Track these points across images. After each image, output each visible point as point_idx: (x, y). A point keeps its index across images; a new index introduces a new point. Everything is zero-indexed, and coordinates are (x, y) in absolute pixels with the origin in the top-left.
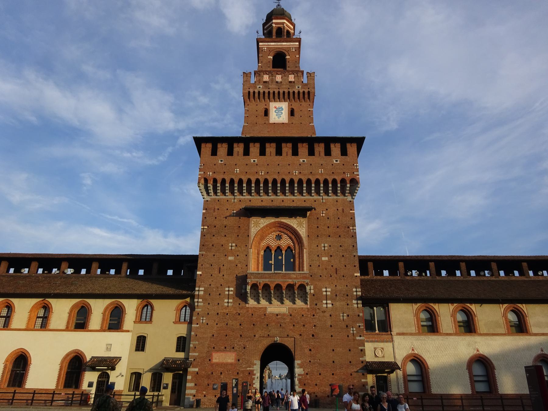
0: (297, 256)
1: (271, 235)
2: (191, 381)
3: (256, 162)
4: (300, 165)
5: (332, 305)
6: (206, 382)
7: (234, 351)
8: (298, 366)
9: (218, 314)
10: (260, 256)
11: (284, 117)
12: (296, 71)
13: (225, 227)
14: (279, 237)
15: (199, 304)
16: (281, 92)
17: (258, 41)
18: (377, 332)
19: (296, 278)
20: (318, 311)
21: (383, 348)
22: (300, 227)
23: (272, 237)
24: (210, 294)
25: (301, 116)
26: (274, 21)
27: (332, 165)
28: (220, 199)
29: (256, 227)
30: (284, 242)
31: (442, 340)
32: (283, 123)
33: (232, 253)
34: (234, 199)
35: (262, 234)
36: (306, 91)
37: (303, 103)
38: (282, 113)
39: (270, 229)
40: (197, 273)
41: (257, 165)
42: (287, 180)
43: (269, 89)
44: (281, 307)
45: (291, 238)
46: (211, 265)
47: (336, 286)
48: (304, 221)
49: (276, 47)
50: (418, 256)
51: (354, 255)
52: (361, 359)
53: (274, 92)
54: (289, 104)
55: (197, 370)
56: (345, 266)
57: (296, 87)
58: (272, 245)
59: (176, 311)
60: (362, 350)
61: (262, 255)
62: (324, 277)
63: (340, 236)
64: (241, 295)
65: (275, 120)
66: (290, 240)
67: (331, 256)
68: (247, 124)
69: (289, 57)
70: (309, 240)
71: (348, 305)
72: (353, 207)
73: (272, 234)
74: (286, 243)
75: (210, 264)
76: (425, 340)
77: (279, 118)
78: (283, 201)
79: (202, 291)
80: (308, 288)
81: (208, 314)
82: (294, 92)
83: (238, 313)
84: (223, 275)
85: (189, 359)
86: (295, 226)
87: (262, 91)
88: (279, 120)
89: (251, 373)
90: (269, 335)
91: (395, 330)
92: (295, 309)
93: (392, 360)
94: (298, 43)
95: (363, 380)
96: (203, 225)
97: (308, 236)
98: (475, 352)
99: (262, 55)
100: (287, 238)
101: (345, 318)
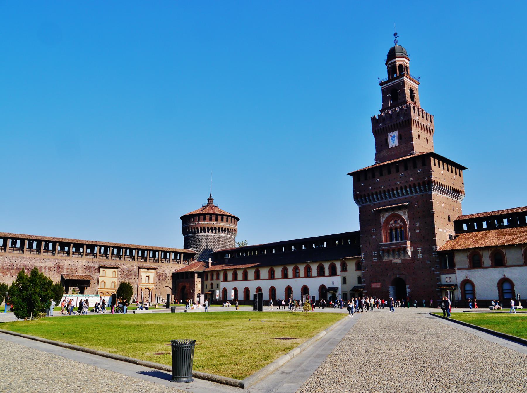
4: (400, 178)
5: (422, 256)
10: (388, 234)
14: (395, 222)
15: (364, 261)
16: (392, 124)
20: (415, 260)
21: (450, 277)
26: (389, 62)
27: (417, 174)
31: (483, 271)
33: (374, 234)
35: (387, 221)
38: (395, 139)
42: (395, 188)
43: (386, 124)
52: (437, 283)
53: (389, 126)
55: (366, 291)
56: (428, 234)
59: (355, 266)
60: (437, 279)
61: (389, 233)
62: (418, 242)
63: (425, 217)
67: (421, 229)
71: (430, 255)
76: (473, 271)
78: (395, 201)
84: (372, 246)
86: (402, 215)
87: (382, 128)
88: (394, 144)
89: (388, 292)
91: (457, 267)
92: (404, 260)
93: (455, 283)
95: (438, 294)
96: (360, 221)
98: (503, 277)
101: (429, 262)
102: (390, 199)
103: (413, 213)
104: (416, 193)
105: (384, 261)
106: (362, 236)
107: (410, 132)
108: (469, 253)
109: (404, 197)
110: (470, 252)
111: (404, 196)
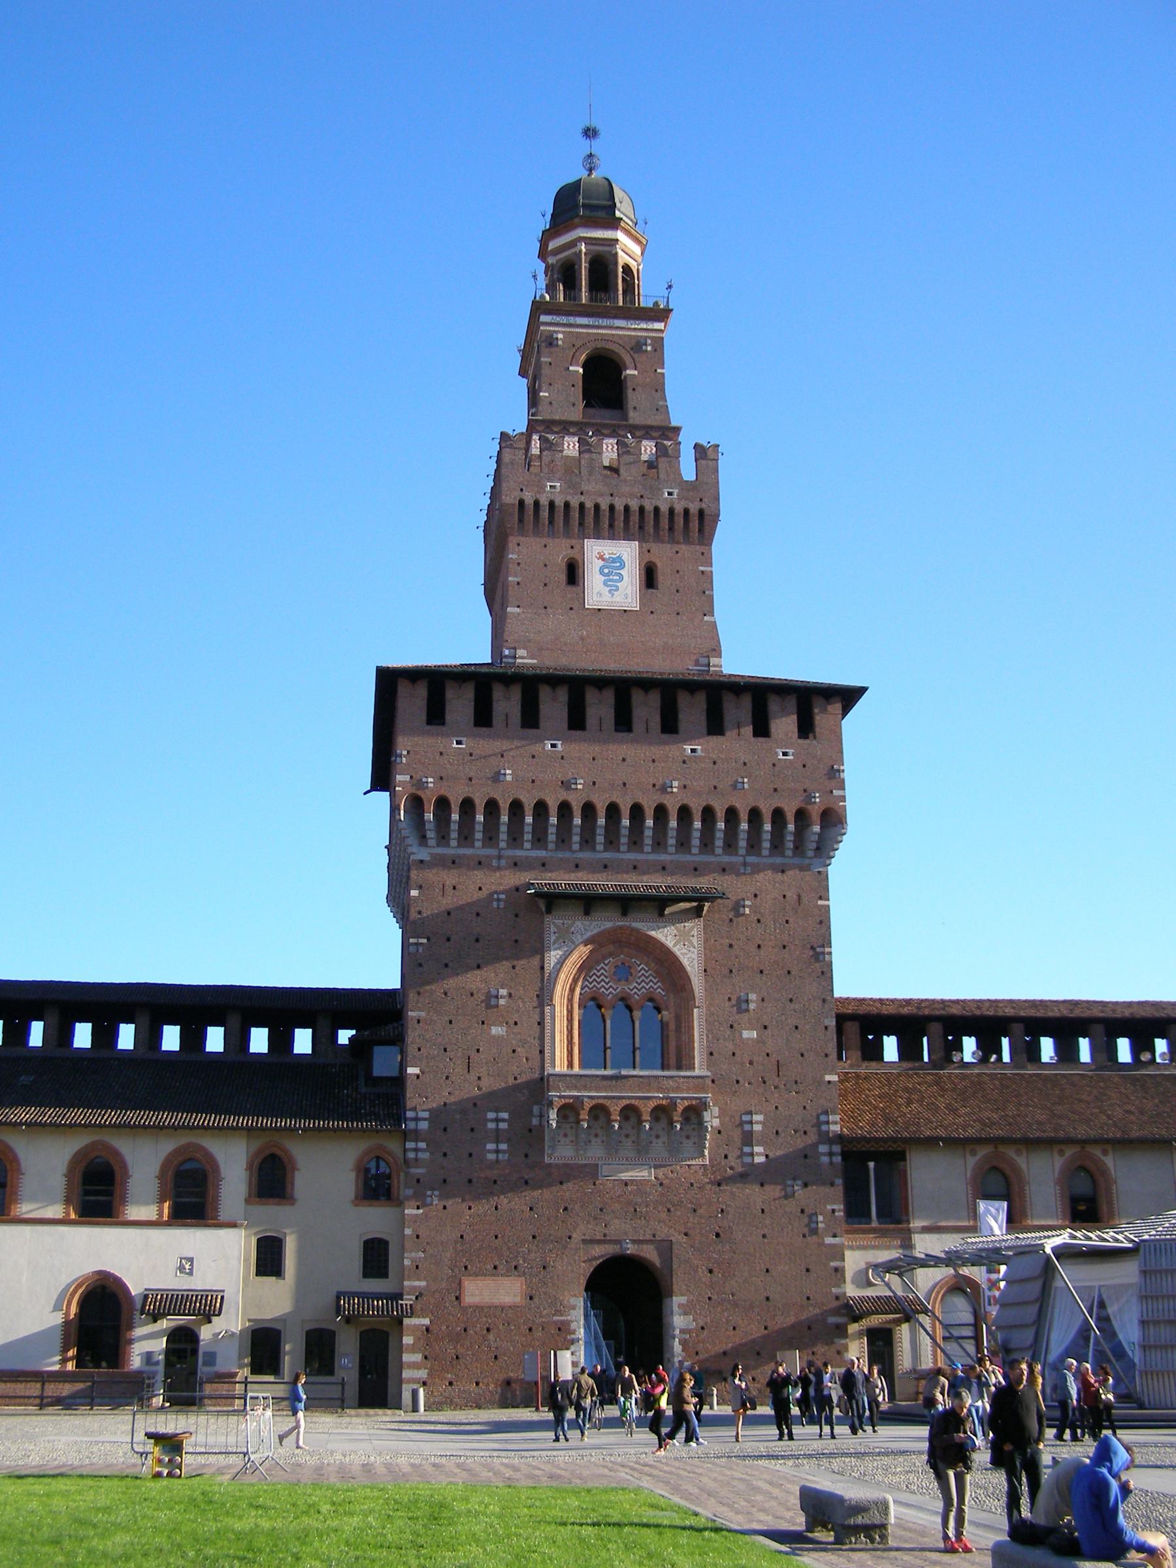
0: (672, 1026)
1: (602, 965)
2: (413, 1349)
3: (560, 748)
5: (767, 1156)
6: (451, 1351)
7: (519, 1276)
8: (680, 1311)
9: (470, 1181)
11: (629, 592)
12: (658, 428)
13: (477, 940)
14: (624, 973)
15: (420, 1155)
16: (619, 507)
17: (538, 308)
18: (875, 1224)
19: (678, 1089)
22: (684, 945)
23: (606, 971)
24: (445, 1130)
25: (677, 591)
27: (774, 765)
28: (459, 856)
29: (564, 942)
30: (639, 984)
32: (625, 611)
34: (499, 859)
36: (694, 508)
37: (683, 548)
39: (602, 947)
40: (408, 1072)
41: (562, 758)
44: (635, 1164)
45: (658, 974)
46: (445, 1050)
47: (777, 1107)
48: (694, 927)
49: (594, 334)
50: (981, 1001)
51: (826, 1025)
52: (834, 1290)
53: (597, 507)
54: (641, 547)
55: (426, 1321)
56: (802, 1055)
57: (663, 493)
58: (607, 993)
59: (354, 1174)
60: (836, 1270)
64: (530, 1131)
65: (601, 599)
66: (653, 979)
68: (518, 610)
69: (636, 373)
70: (707, 981)
72: (826, 888)
73: (606, 962)
74: (643, 987)
75: (442, 1048)
77: (613, 595)
79: (425, 1119)
80: (707, 1116)
81: (445, 1181)
82: (657, 510)
83: (523, 1178)
84: (479, 1078)
85: (405, 1297)
86: (669, 942)
87: (559, 502)
88: (614, 600)
90: (605, 1235)
94: (663, 324)
97: (705, 971)
99: (549, 360)
100: (647, 975)
102: (608, 855)
103: (731, 946)
104: (748, 854)
105: (550, 1165)
106: (423, 1014)
107: (701, 568)
108: (972, 1161)
109: (688, 858)
110: (977, 1158)
111: (690, 852)
